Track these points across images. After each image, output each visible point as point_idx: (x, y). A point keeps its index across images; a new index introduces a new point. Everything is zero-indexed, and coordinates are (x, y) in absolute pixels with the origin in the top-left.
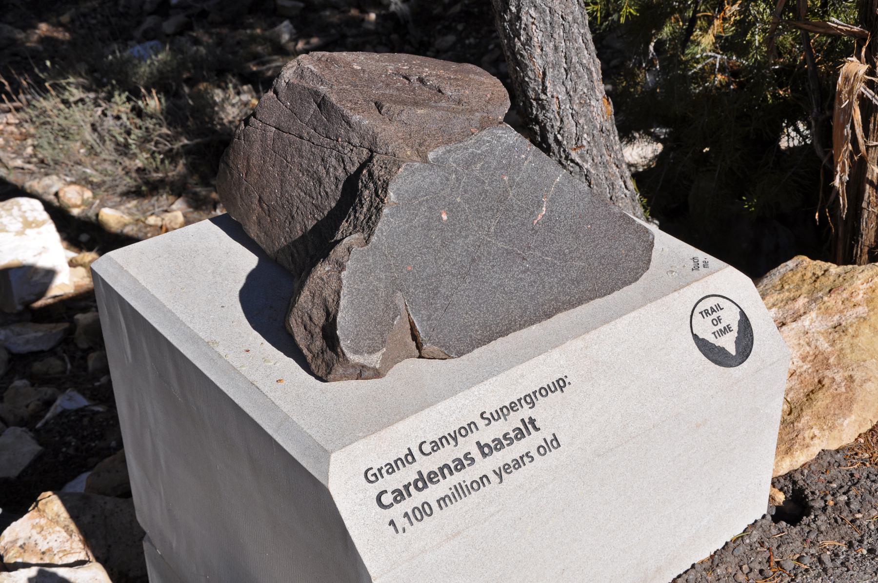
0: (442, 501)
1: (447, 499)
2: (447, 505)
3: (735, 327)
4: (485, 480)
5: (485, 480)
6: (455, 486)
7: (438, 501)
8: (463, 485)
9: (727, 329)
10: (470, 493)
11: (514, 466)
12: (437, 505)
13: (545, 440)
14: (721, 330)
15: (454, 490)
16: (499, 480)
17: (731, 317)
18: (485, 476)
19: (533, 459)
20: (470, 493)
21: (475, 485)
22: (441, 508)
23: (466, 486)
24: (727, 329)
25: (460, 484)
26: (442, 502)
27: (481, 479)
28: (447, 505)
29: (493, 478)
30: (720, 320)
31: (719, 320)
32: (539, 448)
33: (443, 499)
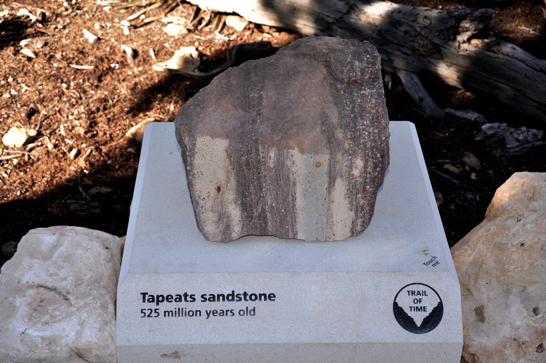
1: (171, 313)
2: (169, 315)
3: (430, 310)
4: (198, 313)
5: (198, 313)
6: (179, 309)
8: (184, 310)
9: (424, 309)
10: (186, 315)
11: (220, 314)
12: (163, 314)
14: (417, 307)
15: (177, 310)
18: (200, 311)
21: (191, 313)
22: (165, 316)
24: (424, 309)
26: (167, 313)
27: (196, 311)
28: (169, 315)
30: (420, 301)
31: (420, 301)
32: (240, 311)
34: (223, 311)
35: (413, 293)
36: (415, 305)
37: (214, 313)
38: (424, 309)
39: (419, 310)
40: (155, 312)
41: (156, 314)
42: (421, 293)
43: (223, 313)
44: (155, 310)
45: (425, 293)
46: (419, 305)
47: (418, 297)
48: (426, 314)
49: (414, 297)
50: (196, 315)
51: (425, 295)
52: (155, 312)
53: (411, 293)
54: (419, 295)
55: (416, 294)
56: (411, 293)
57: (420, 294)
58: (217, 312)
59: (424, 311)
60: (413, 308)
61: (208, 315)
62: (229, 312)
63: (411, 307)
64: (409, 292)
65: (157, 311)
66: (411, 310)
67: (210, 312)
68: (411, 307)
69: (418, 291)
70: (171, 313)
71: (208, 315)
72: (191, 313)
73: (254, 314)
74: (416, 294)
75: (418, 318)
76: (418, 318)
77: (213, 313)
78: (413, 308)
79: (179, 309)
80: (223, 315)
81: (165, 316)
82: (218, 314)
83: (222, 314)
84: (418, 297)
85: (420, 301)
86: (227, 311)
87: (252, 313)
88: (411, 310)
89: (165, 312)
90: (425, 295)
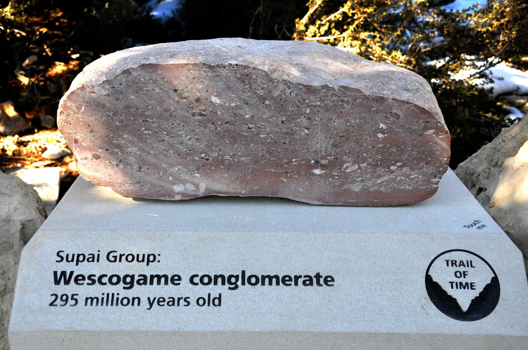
0: (90, 300)
1: (95, 300)
2: (92, 304)
4: (136, 301)
5: (136, 301)
6: (108, 294)
7: (87, 299)
8: (116, 296)
9: (472, 286)
10: (117, 305)
13: (209, 295)
14: (461, 284)
16: (148, 307)
17: (481, 279)
18: (139, 299)
19: (189, 304)
20: (117, 305)
21: (125, 302)
22: (86, 305)
23: (118, 298)
24: (472, 286)
25: (113, 294)
26: (89, 300)
27: (134, 299)
28: (92, 304)
29: (145, 303)
30: (465, 275)
31: (465, 274)
33: (92, 299)
34: (173, 299)
35: (454, 263)
36: (458, 280)
37: (160, 301)
38: (472, 286)
39: (464, 288)
40: (72, 298)
41: (73, 302)
42: (466, 265)
43: (173, 302)
44: (73, 295)
45: (470, 264)
46: (463, 280)
47: (462, 269)
48: (476, 293)
49: (455, 269)
50: (133, 304)
51: (472, 266)
52: (72, 298)
53: (450, 263)
54: (462, 267)
55: (458, 264)
56: (450, 263)
57: (464, 265)
58: (164, 301)
59: (472, 289)
60: (454, 285)
61: (151, 305)
62: (182, 302)
63: (452, 283)
64: (447, 261)
65: (75, 297)
66: (452, 288)
67: (155, 299)
68: (452, 283)
69: (461, 261)
70: (95, 300)
71: (151, 305)
72: (125, 302)
73: (220, 304)
74: (458, 264)
75: (464, 299)
76: (464, 299)
77: (159, 302)
78: (454, 285)
79: (108, 294)
80: (173, 304)
81: (86, 305)
82: (166, 303)
83: (171, 303)
84: (462, 269)
85: (465, 274)
86: (179, 299)
87: (217, 302)
88: (452, 288)
89: (87, 299)
90: (472, 266)
